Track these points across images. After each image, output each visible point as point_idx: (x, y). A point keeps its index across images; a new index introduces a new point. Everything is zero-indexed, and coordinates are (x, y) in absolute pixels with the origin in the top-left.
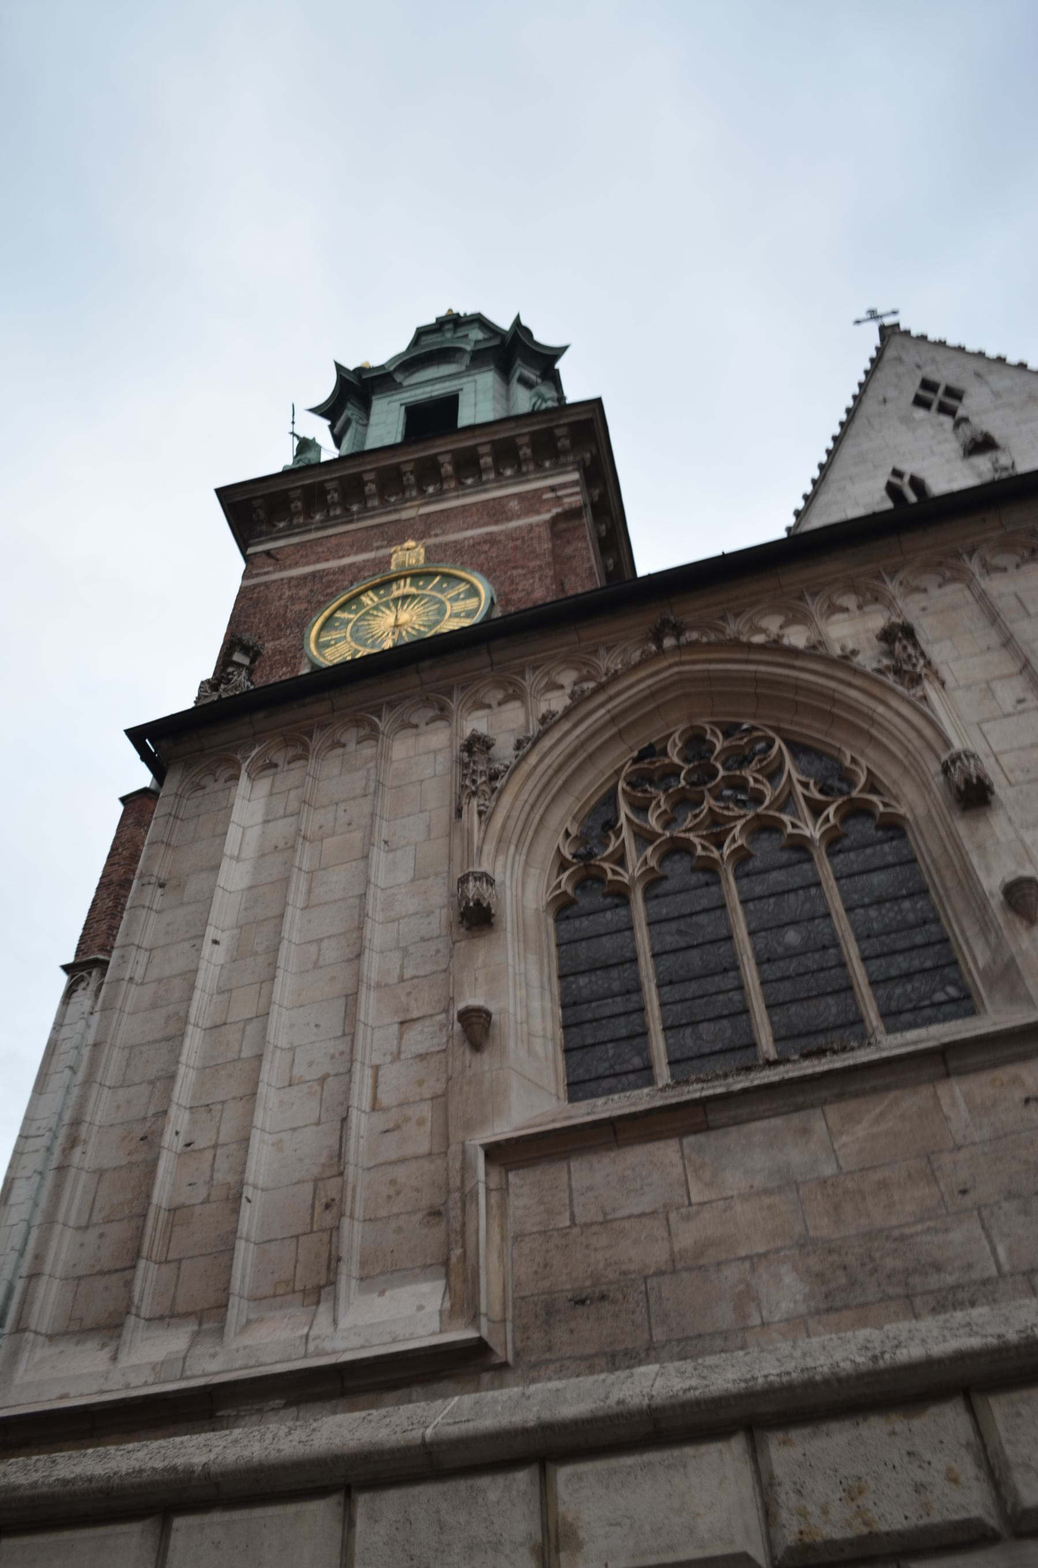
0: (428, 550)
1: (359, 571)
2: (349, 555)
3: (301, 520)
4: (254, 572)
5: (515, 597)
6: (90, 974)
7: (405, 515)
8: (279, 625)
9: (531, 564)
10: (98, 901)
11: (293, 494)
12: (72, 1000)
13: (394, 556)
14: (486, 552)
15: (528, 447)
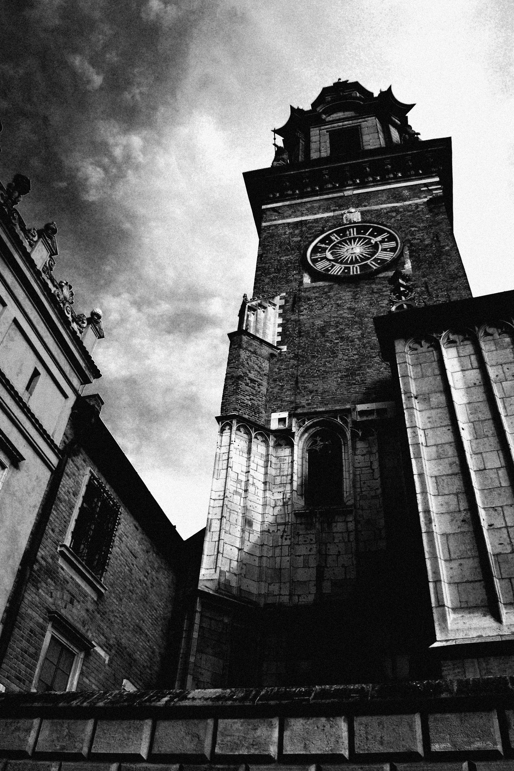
0: (362, 213)
2: (319, 213)
10: (228, 386)
14: (394, 217)
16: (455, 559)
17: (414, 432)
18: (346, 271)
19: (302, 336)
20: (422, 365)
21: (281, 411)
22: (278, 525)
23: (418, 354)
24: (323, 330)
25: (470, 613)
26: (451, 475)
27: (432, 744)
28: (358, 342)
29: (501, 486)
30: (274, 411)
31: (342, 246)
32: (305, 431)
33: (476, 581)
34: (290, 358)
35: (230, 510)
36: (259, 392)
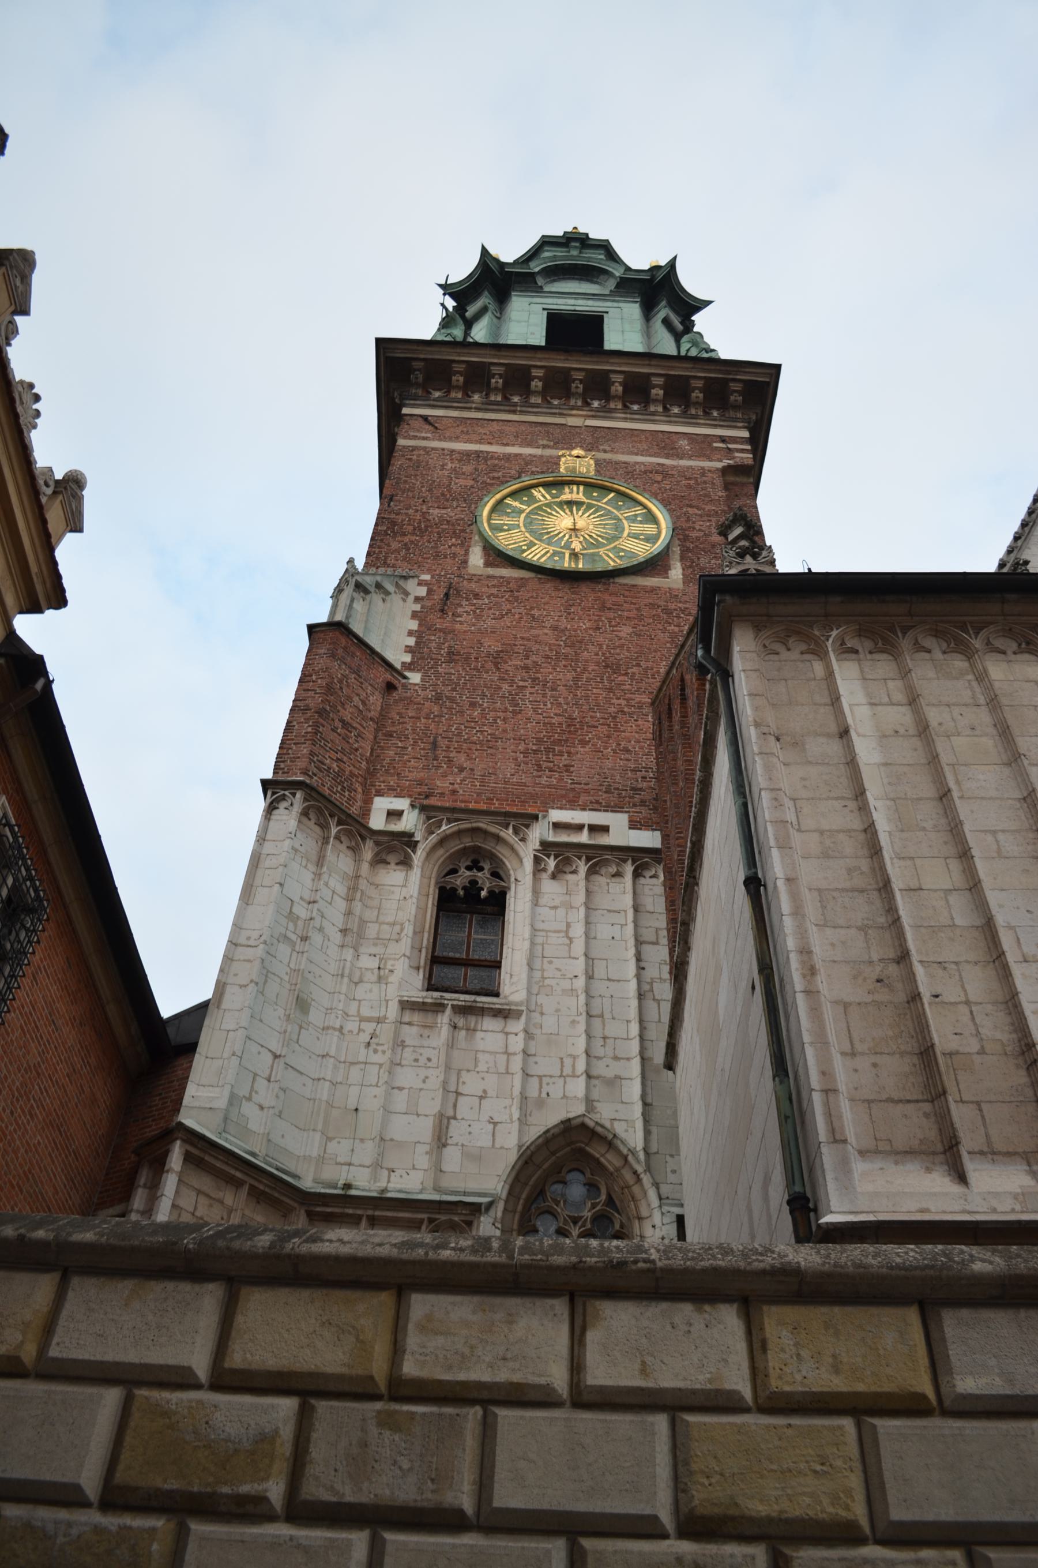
0: (598, 463)
1: (527, 464)
2: (513, 445)
3: (460, 395)
4: (412, 434)
5: (694, 534)
6: (294, 795)
7: (571, 421)
8: (443, 494)
9: (708, 507)
10: (295, 723)
11: (457, 367)
12: (273, 817)
13: (563, 459)
14: (658, 482)
15: (621, 385)
16: (863, 1054)
17: (776, 799)
18: (556, 558)
19: (456, 661)
20: (789, 682)
21: (395, 797)
22: (360, 1021)
23: (780, 661)
24: (497, 659)
25: (896, 1163)
26: (853, 890)
27: (958, 1377)
28: (565, 693)
29: (954, 925)
30: (379, 793)
31: (554, 513)
32: (442, 842)
33: (909, 1101)
34: (426, 699)
35: (268, 971)
36: (357, 750)
